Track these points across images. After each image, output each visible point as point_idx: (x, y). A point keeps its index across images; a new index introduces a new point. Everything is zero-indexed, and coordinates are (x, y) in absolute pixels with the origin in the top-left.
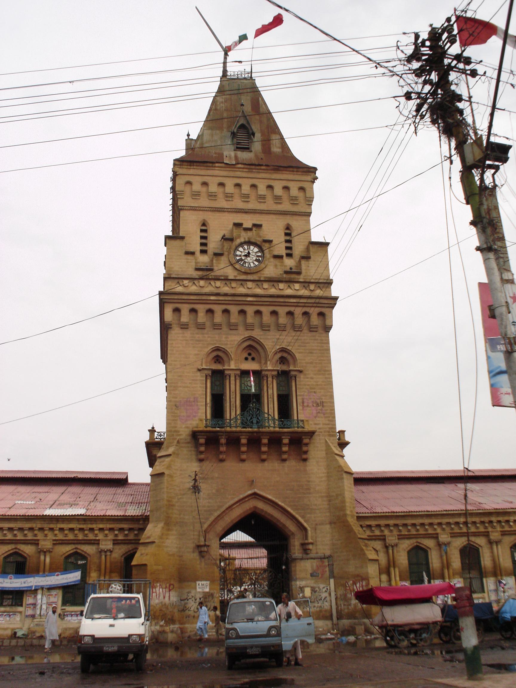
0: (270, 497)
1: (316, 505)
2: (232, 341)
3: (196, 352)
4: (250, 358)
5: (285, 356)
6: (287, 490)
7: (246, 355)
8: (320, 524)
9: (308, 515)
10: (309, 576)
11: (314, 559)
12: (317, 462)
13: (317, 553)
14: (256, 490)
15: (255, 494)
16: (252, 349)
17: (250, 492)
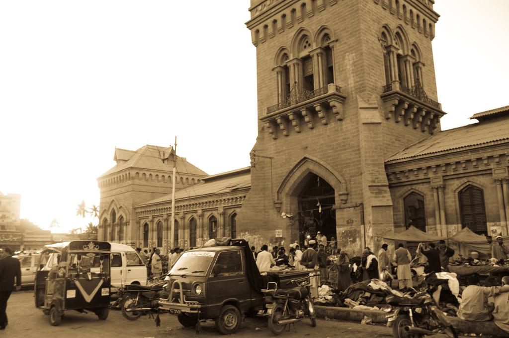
0: (315, 159)
1: (349, 159)
2: (288, 38)
3: (270, 58)
4: (307, 45)
5: (324, 34)
6: (329, 150)
7: (305, 44)
8: (353, 176)
9: (344, 170)
10: (345, 223)
11: (349, 208)
12: (351, 119)
13: (351, 202)
14: (307, 156)
15: (305, 158)
16: (303, 38)
17: (303, 157)
